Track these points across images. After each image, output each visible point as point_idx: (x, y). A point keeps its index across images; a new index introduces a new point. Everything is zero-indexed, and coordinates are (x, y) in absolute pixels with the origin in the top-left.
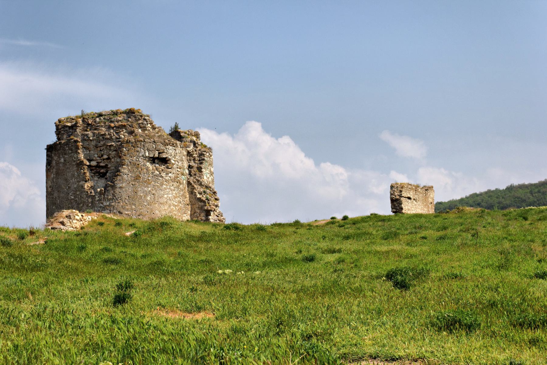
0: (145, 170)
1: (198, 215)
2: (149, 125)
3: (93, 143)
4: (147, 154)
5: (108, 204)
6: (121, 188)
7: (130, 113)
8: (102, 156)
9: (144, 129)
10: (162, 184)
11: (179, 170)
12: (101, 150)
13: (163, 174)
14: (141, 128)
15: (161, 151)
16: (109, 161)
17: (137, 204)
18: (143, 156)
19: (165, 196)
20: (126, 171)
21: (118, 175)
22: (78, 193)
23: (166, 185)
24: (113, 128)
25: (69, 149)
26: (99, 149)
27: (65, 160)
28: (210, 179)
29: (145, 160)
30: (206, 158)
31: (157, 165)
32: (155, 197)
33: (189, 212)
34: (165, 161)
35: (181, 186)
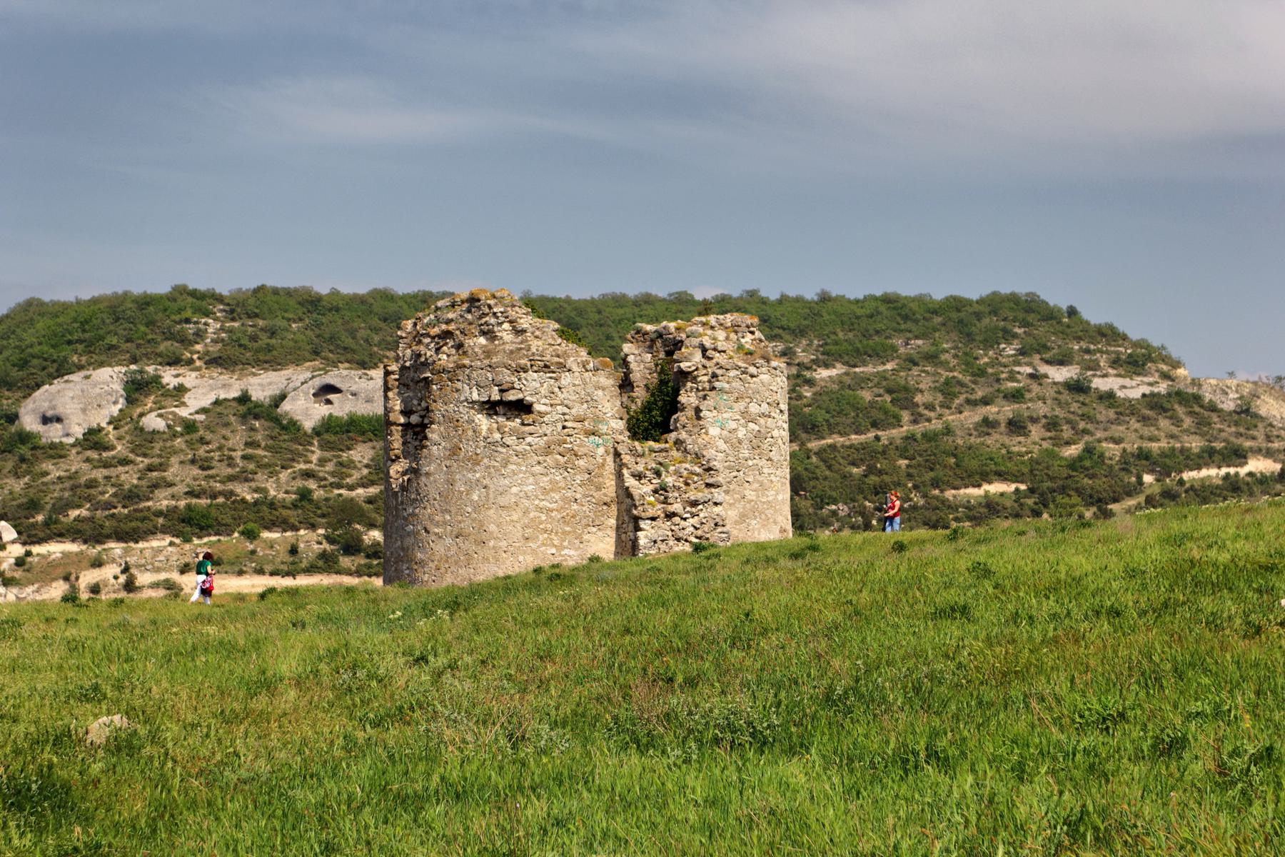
0: (470, 433)
6: (427, 474)
9: (489, 334)
10: (506, 463)
13: (510, 440)
14: (483, 333)
15: (504, 387)
17: (453, 510)
19: (515, 490)
21: (425, 447)
23: (518, 464)
31: (501, 419)
33: (613, 522)
34: (522, 408)
35: (581, 463)
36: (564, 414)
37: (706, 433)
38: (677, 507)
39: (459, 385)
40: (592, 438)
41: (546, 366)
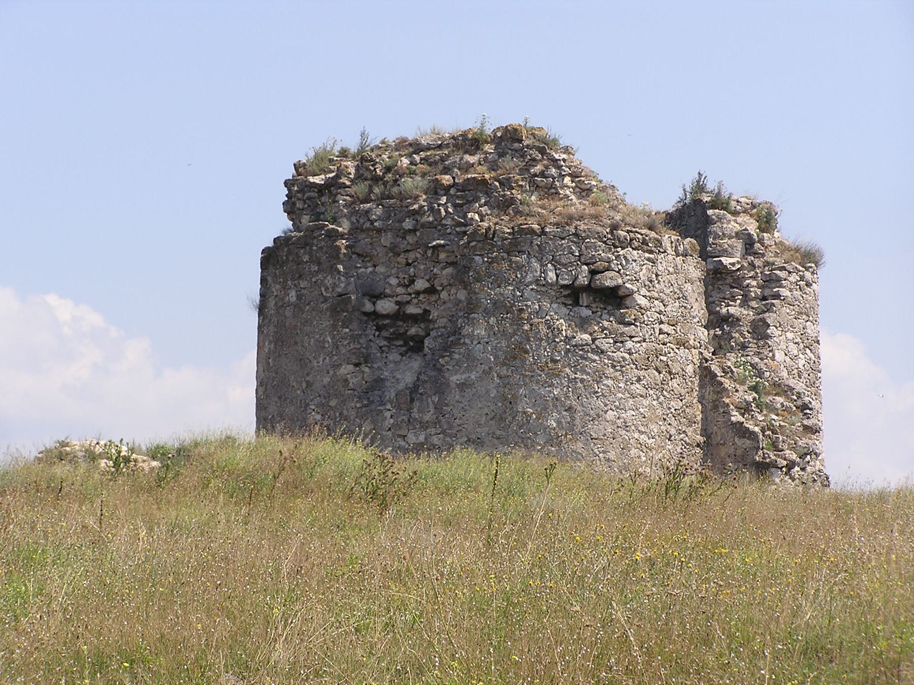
0: (543, 329)
2: (567, 180)
3: (387, 239)
4: (552, 276)
5: (422, 438)
6: (462, 386)
7: (509, 138)
8: (412, 282)
10: (599, 377)
11: (665, 328)
12: (408, 264)
13: (605, 343)
15: (600, 265)
16: (433, 298)
18: (537, 281)
19: (611, 415)
20: (481, 331)
22: (333, 403)
24: (447, 189)
25: (311, 261)
26: (401, 259)
27: (299, 297)
28: (801, 362)
29: (543, 293)
30: (785, 292)
32: (573, 419)
34: (614, 299)
35: (674, 384)
36: (660, 313)
39: (522, 259)
41: (644, 242)
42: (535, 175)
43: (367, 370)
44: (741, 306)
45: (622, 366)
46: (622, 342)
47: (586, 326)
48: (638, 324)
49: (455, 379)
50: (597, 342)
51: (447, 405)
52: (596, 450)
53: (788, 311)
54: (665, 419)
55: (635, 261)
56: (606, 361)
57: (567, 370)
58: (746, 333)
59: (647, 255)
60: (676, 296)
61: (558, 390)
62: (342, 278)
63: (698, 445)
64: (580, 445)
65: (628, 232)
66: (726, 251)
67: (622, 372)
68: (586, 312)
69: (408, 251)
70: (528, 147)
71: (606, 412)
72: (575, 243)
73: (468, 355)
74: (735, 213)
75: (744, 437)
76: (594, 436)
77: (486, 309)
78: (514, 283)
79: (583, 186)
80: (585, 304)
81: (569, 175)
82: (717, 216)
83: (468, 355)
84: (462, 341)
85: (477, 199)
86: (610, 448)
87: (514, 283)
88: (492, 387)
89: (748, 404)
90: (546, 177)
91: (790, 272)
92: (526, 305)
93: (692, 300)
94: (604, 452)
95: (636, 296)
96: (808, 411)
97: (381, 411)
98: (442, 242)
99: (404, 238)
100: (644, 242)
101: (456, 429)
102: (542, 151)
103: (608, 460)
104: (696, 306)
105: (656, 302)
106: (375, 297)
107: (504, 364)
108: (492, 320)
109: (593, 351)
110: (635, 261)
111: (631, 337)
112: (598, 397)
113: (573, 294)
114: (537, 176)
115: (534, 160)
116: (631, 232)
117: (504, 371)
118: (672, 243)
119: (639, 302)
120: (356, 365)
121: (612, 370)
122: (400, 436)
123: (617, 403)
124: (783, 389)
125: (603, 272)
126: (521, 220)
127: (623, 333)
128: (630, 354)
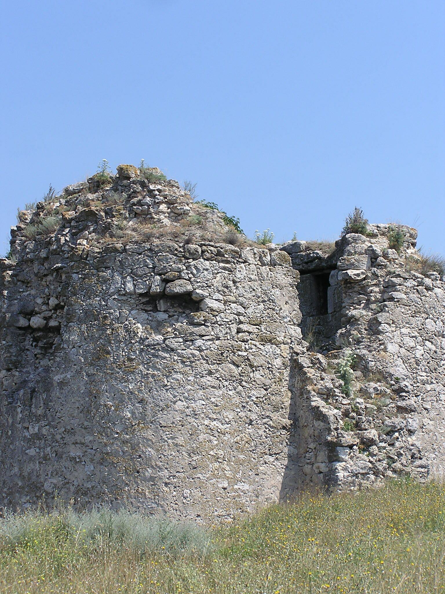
0: (122, 332)
1: (313, 460)
4: (130, 286)
6: (62, 384)
10: (169, 372)
13: (174, 343)
15: (170, 275)
20: (74, 337)
34: (189, 303)
35: (257, 375)
36: (239, 314)
37: (385, 350)
38: (372, 433)
39: (107, 274)
40: (268, 347)
41: (219, 254)
42: (134, 204)
43: (17, 374)
44: (364, 308)
45: (191, 362)
46: (192, 341)
47: (160, 328)
48: (209, 324)
49: (57, 378)
50: (167, 342)
51: (51, 401)
52: (165, 437)
53: (403, 310)
54: (244, 407)
55: (207, 270)
56: (176, 358)
57: (141, 367)
58: (363, 330)
59: (222, 265)
60: (260, 299)
61: (133, 385)
62: (6, 301)
63: (284, 428)
64: (150, 432)
65: (201, 246)
66: (353, 264)
67: (192, 367)
68: (162, 316)
69: (46, 275)
70: (134, 182)
71: (175, 403)
72: (150, 257)
73: (66, 357)
74: (373, 236)
75: (319, 420)
76: (163, 424)
77: (79, 317)
78: (101, 294)
79: (176, 211)
80: (162, 309)
81: (166, 203)
82: (353, 238)
83: (66, 357)
84: (62, 346)
85: (86, 228)
86: (178, 435)
87: (101, 294)
88: (81, 384)
89: (329, 390)
90: (142, 206)
91: (405, 279)
92: (109, 313)
93: (282, 303)
94: (172, 438)
95: (207, 300)
96: (404, 394)
97: (16, 407)
98: (60, 265)
99: (43, 265)
100: (219, 254)
101: (57, 421)
102: (143, 185)
103: (177, 445)
104: (286, 307)
105: (233, 305)
106: (29, 314)
107: (91, 364)
108: (84, 327)
109: (164, 350)
110: (207, 270)
111: (201, 336)
112: (167, 390)
113: (150, 301)
114: (135, 205)
115: (135, 192)
116: (205, 245)
117: (92, 371)
118: (255, 254)
119: (210, 305)
120: (9, 370)
121: (181, 365)
122: (25, 428)
123: (186, 395)
124: (384, 376)
125: (174, 281)
126: (108, 239)
127: (193, 332)
128: (201, 350)
